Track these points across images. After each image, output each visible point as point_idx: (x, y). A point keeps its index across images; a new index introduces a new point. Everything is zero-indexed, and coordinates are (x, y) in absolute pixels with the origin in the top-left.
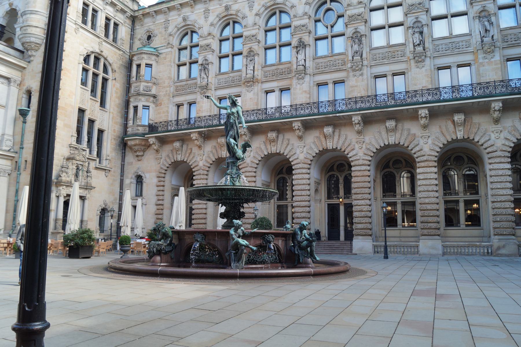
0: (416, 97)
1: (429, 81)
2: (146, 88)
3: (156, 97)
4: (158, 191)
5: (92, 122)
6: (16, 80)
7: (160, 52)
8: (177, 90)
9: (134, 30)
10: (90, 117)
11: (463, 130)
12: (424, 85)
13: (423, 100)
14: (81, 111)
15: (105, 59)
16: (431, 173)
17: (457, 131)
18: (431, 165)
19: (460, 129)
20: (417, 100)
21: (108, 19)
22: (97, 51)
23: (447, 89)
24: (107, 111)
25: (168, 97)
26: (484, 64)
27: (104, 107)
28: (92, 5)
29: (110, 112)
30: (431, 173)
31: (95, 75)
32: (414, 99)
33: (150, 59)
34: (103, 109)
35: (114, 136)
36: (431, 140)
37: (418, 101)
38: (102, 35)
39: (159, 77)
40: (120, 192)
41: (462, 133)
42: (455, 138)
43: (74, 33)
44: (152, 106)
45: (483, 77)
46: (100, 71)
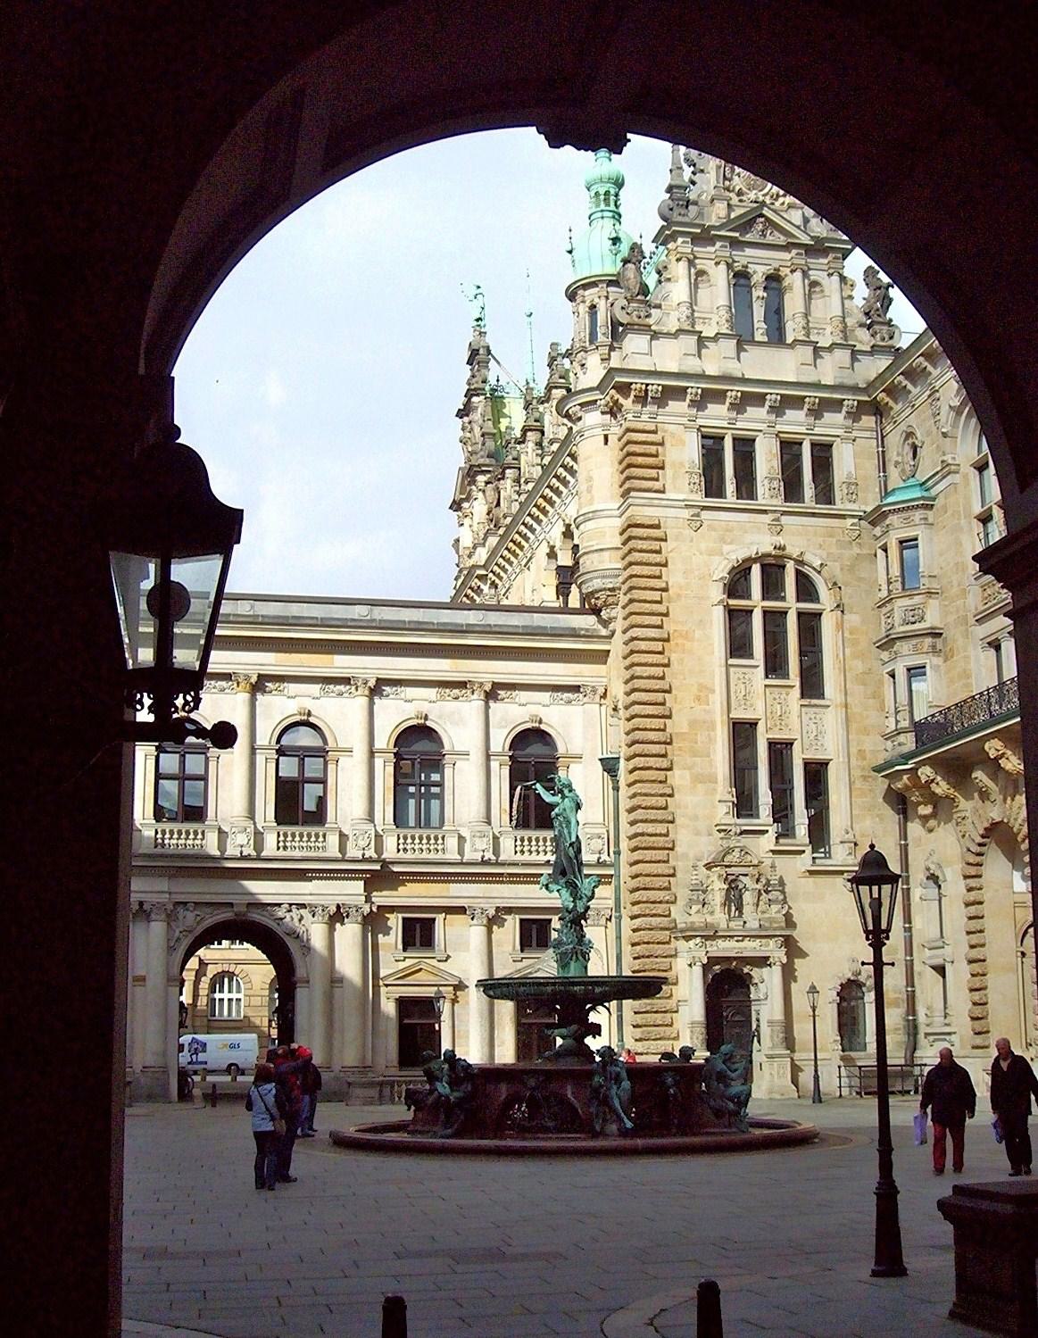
2: (911, 613)
3: (941, 634)
4: (970, 918)
5: (780, 751)
6: (593, 687)
7: (933, 492)
8: (986, 600)
9: (883, 437)
10: (771, 736)
14: (742, 733)
15: (800, 562)
21: (789, 448)
22: (769, 549)
24: (828, 703)
25: (963, 628)
27: (821, 696)
28: (730, 432)
29: (836, 706)
31: (774, 620)
33: (909, 523)
34: (815, 701)
35: (863, 769)
38: (774, 502)
39: (941, 568)
40: (906, 930)
43: (688, 532)
44: (930, 661)
46: (791, 603)
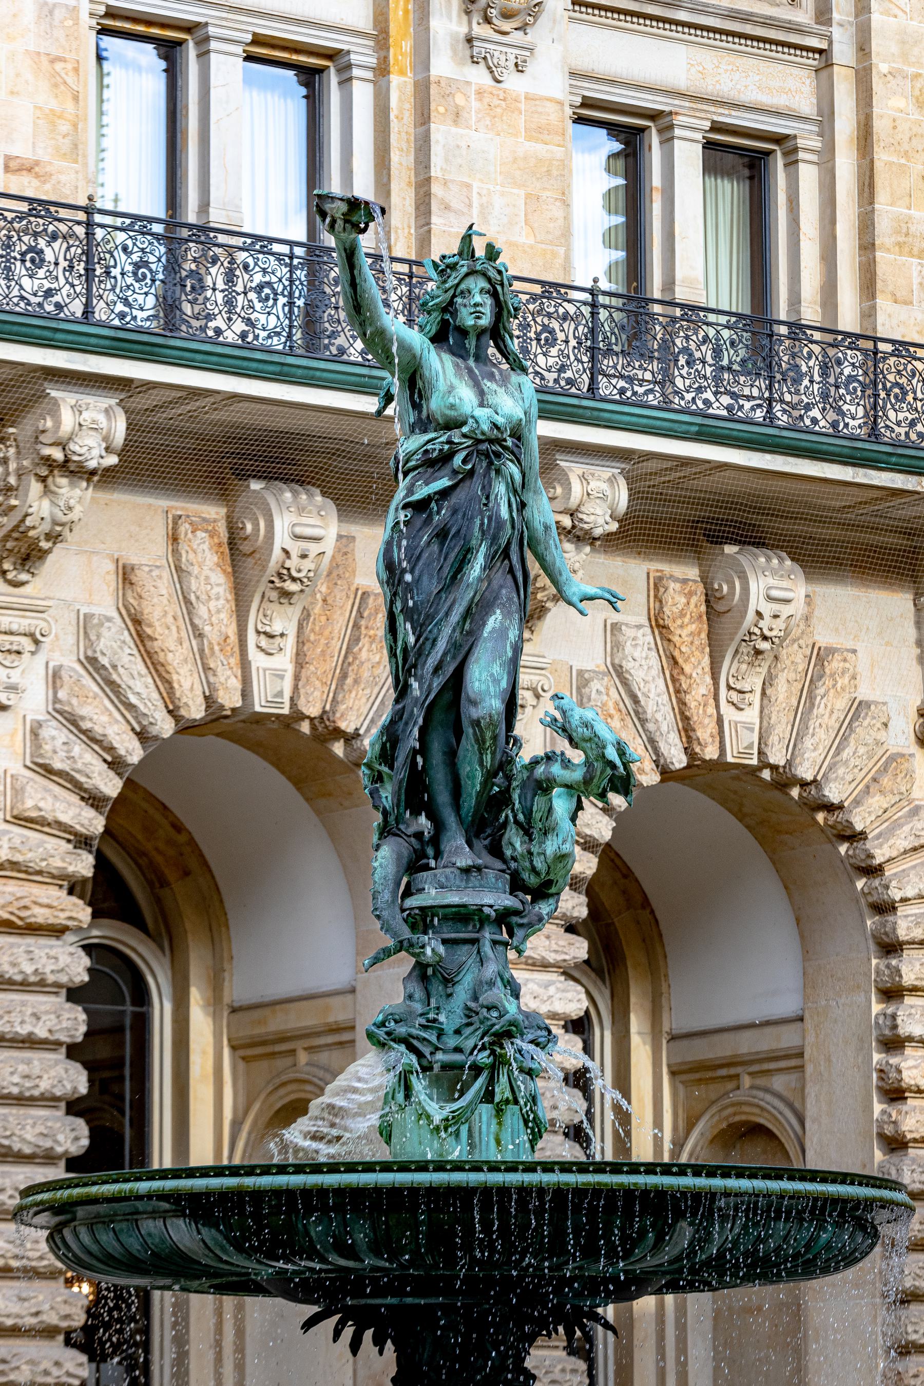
0: (38, 261)
1: (64, 127)
11: (290, 644)
12: (21, 150)
13: (88, 311)
16: (39, 985)
17: (251, 637)
18: (40, 915)
19: (277, 628)
20: (49, 293)
23: (279, 257)
26: (460, 100)
30: (39, 985)
32: (26, 282)
36: (55, 677)
37: (58, 306)
41: (284, 662)
42: (230, 699)
45: (447, 208)
